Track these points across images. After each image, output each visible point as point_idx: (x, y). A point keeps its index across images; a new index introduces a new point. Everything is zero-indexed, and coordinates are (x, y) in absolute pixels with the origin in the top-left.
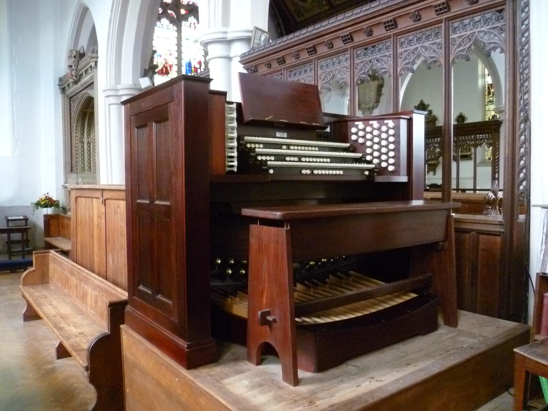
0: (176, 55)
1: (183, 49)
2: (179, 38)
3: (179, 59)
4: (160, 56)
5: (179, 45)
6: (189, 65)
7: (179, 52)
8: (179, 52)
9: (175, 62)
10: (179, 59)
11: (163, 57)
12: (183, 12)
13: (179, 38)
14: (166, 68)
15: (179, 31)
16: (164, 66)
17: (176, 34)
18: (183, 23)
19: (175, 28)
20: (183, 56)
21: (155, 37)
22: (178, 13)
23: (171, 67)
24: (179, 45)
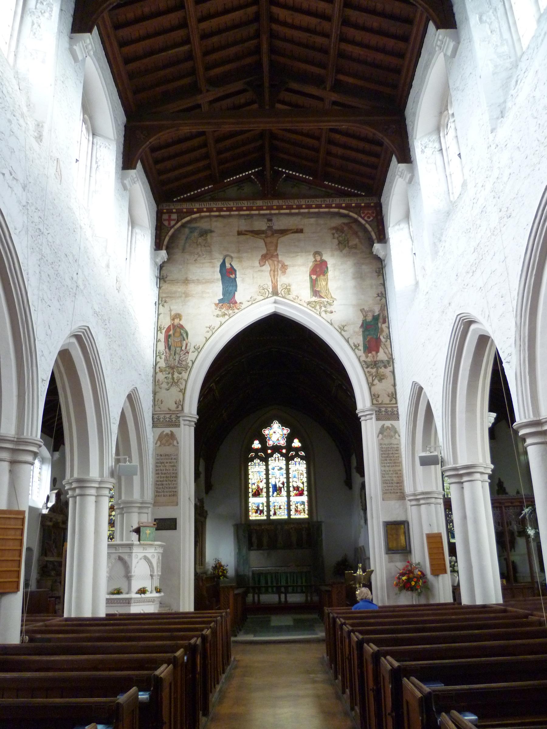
0: (265, 481)
1: (270, 476)
2: (267, 470)
3: (268, 483)
5: (267, 474)
7: (267, 479)
8: (267, 479)
9: (265, 486)
10: (268, 483)
11: (256, 485)
12: (269, 451)
13: (267, 470)
14: (258, 491)
15: (267, 465)
16: (257, 490)
17: (264, 467)
20: (270, 481)
21: (250, 472)
22: (265, 452)
23: (262, 490)
24: (267, 474)
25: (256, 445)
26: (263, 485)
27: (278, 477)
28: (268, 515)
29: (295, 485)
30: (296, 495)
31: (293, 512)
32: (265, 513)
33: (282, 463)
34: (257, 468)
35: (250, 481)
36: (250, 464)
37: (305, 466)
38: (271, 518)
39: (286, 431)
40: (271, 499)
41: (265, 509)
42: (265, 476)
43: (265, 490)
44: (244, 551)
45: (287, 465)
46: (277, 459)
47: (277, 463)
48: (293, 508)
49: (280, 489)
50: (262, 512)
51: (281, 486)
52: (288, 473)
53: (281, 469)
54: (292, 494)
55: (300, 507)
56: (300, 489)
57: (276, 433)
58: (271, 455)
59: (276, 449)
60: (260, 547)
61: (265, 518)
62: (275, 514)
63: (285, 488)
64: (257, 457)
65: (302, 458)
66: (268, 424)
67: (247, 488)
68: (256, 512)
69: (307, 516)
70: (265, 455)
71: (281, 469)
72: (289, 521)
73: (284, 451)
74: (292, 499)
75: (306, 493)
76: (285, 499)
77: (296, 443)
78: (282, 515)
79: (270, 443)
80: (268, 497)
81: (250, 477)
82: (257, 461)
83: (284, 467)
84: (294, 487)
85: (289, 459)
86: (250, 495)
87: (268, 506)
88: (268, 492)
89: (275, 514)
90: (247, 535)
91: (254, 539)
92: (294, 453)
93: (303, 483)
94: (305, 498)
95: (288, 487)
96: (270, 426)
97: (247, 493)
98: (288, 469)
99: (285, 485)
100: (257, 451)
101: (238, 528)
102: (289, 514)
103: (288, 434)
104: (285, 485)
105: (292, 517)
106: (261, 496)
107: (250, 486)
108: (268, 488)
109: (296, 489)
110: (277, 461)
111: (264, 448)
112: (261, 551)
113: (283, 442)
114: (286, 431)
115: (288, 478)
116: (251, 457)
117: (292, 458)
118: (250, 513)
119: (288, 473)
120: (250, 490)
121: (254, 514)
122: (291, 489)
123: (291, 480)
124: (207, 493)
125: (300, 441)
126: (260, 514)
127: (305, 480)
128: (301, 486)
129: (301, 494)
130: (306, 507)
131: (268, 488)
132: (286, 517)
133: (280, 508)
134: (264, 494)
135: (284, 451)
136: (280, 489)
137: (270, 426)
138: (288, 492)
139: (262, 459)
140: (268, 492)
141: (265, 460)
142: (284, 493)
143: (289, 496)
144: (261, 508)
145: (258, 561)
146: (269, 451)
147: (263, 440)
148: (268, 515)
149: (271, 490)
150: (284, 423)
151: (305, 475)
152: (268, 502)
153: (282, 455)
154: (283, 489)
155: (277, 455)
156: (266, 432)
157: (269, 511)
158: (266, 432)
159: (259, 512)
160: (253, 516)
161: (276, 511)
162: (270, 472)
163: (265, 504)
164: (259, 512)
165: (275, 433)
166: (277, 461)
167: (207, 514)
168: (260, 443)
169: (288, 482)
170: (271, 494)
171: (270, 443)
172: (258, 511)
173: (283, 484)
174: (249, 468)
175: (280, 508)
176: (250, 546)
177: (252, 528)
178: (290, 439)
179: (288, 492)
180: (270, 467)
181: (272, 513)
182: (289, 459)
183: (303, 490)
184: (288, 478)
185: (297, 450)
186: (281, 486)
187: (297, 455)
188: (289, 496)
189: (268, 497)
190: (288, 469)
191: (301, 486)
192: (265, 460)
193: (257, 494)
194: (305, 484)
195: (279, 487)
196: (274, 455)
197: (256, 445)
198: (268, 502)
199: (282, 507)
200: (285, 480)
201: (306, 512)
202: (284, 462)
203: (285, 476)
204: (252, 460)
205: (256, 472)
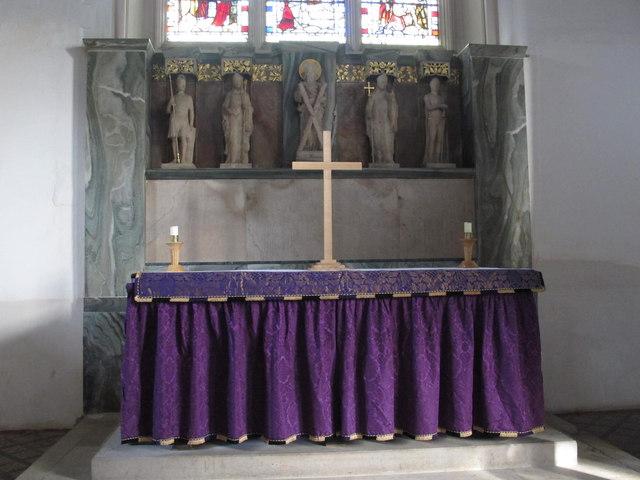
28: (256, 27)
32: (243, 19)
44: (125, 175)
60: (212, 156)
62: (288, 22)
89: (288, 22)
90: (141, 100)
91: (183, 125)
101: (92, 56)
102: (354, 28)
105: (366, 40)
112: (214, 184)
118: (172, 15)
126: (219, 20)
145: (190, 229)
148: (256, 27)
176: (162, 151)
177: (172, 68)
181: (273, 18)
201: (433, 23)
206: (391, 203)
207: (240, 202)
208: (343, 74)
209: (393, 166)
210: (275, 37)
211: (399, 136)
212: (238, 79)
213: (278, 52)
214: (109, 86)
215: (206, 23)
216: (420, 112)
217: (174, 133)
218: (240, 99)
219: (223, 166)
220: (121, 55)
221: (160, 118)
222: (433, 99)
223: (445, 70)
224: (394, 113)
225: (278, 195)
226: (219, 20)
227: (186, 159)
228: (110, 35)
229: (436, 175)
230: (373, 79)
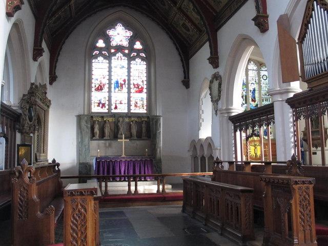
0: (107, 77)
1: (112, 74)
2: (110, 68)
3: (110, 80)
4: (97, 80)
5: (110, 71)
6: (117, 82)
7: (110, 75)
8: (110, 75)
9: (107, 82)
10: (110, 80)
11: (99, 80)
13: (110, 68)
14: (101, 86)
15: (110, 63)
17: (108, 65)
18: (113, 58)
19: (107, 61)
20: (112, 78)
23: (104, 85)
24: (110, 71)
25: (101, 44)
26: (106, 81)
27: (119, 74)
28: (109, 109)
29: (135, 83)
30: (137, 92)
31: (132, 107)
32: (107, 107)
33: (125, 62)
34: (100, 65)
35: (93, 77)
36: (94, 61)
37: (145, 66)
38: (112, 111)
39: (129, 34)
40: (113, 94)
41: (107, 103)
42: (108, 73)
43: (107, 86)
45: (129, 64)
46: (119, 58)
47: (119, 61)
48: (133, 103)
49: (122, 85)
50: (103, 105)
51: (123, 83)
52: (129, 72)
53: (123, 67)
54: (133, 90)
55: (140, 104)
56: (140, 87)
57: (120, 35)
58: (114, 54)
59: (120, 48)
60: (102, 136)
61: (107, 111)
62: (116, 108)
63: (127, 85)
64: (101, 54)
65: (143, 59)
66: (112, 25)
67: (90, 83)
68: (98, 106)
69: (145, 112)
70: (110, 52)
71: (123, 67)
72: (129, 115)
73: (127, 51)
74: (132, 95)
75: (145, 90)
76: (126, 95)
77: (138, 45)
78: (123, 109)
79: (114, 43)
80: (110, 91)
81: (93, 73)
82: (101, 59)
83: (126, 66)
84: (134, 85)
85: (130, 59)
86: (93, 89)
87: (110, 100)
88: (110, 88)
89: (116, 108)
91: (97, 130)
92: (135, 54)
93: (143, 81)
94: (144, 95)
95: (129, 84)
96: (115, 28)
97: (90, 87)
98: (129, 68)
99: (127, 83)
100: (101, 49)
101: (79, 118)
103: (131, 37)
104: (127, 83)
105: (132, 111)
106: (103, 91)
107: (93, 81)
108: (110, 84)
109: (136, 86)
110: (119, 60)
111: (108, 47)
113: (125, 43)
114: (129, 34)
115: (129, 76)
116: (96, 55)
117: (134, 58)
118: (93, 106)
119: (129, 72)
120: (93, 85)
121: (96, 107)
122: (132, 86)
123: (132, 78)
124: (51, 83)
125: (142, 44)
126: (102, 107)
127: (145, 79)
128: (141, 84)
129: (141, 91)
130: (145, 103)
131: (110, 84)
132: (127, 111)
133: (121, 103)
134: (106, 89)
135: (127, 51)
136: (122, 85)
137: (115, 28)
138: (129, 88)
139: (105, 57)
140: (110, 88)
141: (108, 58)
142: (125, 89)
143: (129, 92)
144: (103, 102)
145: (98, 150)
146: (113, 51)
147: (107, 39)
148: (109, 109)
149: (113, 86)
150: (127, 26)
151: (145, 75)
152: (110, 97)
153: (125, 55)
154: (124, 86)
155: (119, 55)
156: (111, 32)
157: (110, 105)
158: (111, 32)
159: (101, 105)
160: (95, 109)
161: (117, 105)
162: (112, 70)
163: (107, 99)
164: (101, 105)
165: (118, 34)
166: (119, 60)
167: (50, 104)
168: (105, 42)
169: (129, 80)
170: (113, 89)
171: (114, 43)
172: (100, 104)
173: (124, 81)
174: (93, 64)
175: (121, 103)
177: (94, 119)
178: (132, 41)
179: (129, 88)
180: (113, 65)
181: (113, 107)
182: (130, 59)
183: (142, 88)
184: (129, 76)
185: (138, 51)
186: (123, 83)
187: (138, 56)
188: (129, 92)
189: (110, 91)
190: (129, 68)
191: (141, 84)
192: (108, 58)
193: (100, 88)
194: (145, 83)
195: (121, 84)
196: (117, 55)
197: (101, 44)
198: (110, 97)
199: (123, 102)
200: (126, 78)
201: (145, 108)
202: (126, 61)
203: (127, 74)
204: (96, 57)
205: (99, 68)
206: (135, 145)
207: (108, 144)
208: (127, 120)
209: (136, 138)
210: (114, 111)
211: (137, 132)
212: (107, 121)
213: (114, 115)
214: (83, 123)
215: (99, 108)
216: (141, 127)
217: (95, 132)
218: (107, 125)
219: (104, 138)
220: (86, 117)
221: (92, 129)
222: (143, 125)
223: (146, 119)
224: (136, 128)
225: (114, 143)
226: (102, 107)
227: (97, 136)
228: (82, 113)
229: (144, 140)
230: (132, 121)
